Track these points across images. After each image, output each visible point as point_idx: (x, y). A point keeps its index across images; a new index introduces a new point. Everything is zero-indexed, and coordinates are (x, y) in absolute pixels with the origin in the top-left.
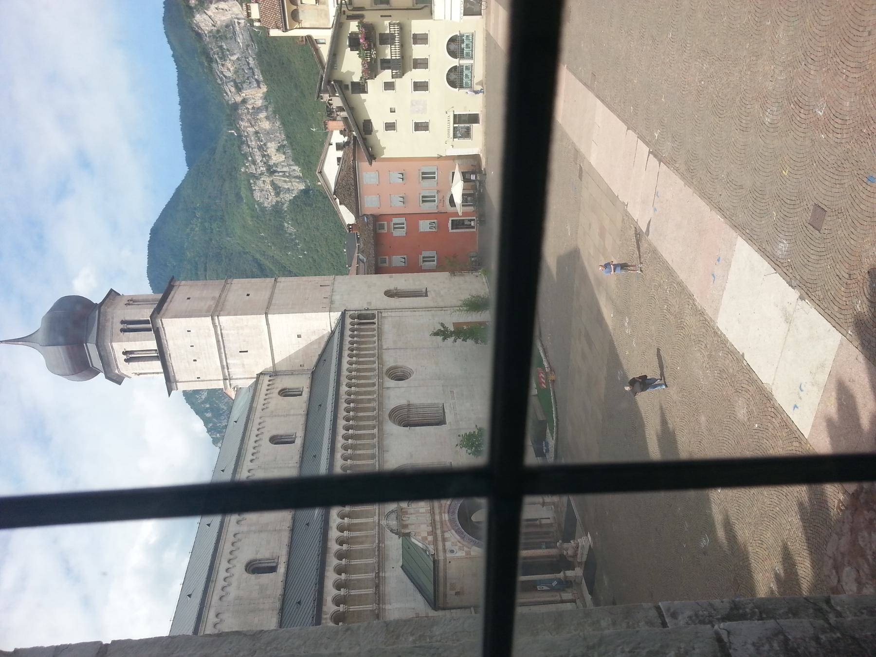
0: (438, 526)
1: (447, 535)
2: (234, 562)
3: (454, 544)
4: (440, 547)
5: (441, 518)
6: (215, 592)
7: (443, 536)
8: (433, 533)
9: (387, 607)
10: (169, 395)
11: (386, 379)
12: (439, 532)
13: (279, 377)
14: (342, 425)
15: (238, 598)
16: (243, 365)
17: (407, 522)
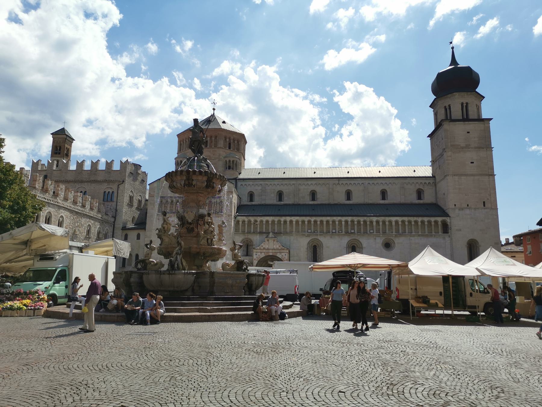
0: (267, 251)
1: (263, 254)
2: (316, 185)
3: (259, 255)
4: (258, 251)
5: (270, 252)
6: (302, 182)
7: (263, 252)
8: (264, 249)
9: (258, 236)
10: (428, 137)
11: (384, 238)
12: (265, 251)
13: (434, 188)
14: (348, 219)
15: (299, 190)
16: (437, 169)
17: (270, 241)
